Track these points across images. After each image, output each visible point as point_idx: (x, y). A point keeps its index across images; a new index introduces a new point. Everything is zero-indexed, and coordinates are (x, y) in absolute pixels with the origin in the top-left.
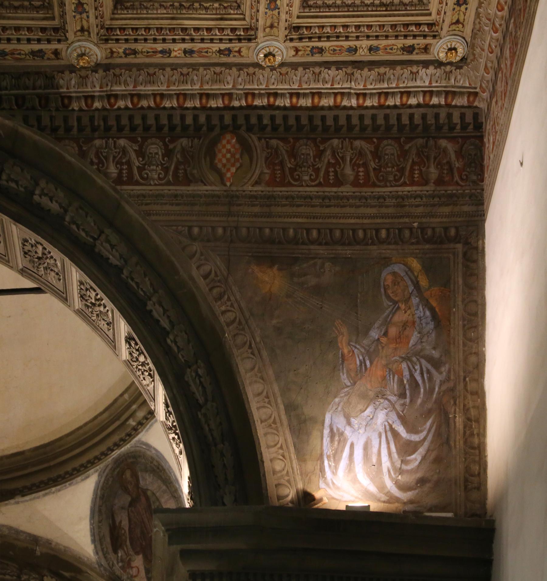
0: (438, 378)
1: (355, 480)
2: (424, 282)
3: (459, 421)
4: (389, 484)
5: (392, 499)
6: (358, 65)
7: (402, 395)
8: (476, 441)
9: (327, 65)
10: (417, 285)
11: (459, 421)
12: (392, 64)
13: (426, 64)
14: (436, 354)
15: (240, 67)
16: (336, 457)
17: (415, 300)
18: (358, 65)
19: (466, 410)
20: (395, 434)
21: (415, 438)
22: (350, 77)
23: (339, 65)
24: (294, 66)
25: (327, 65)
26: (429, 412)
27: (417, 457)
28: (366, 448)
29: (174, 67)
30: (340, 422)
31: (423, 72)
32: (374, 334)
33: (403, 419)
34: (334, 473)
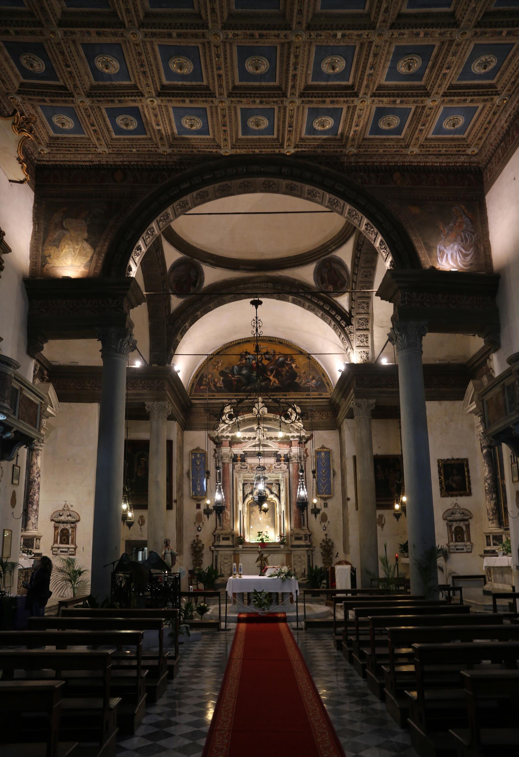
0: (474, 237)
1: (449, 264)
2: (466, 211)
3: (482, 248)
4: (460, 265)
5: (461, 269)
6: (441, 155)
7: (462, 241)
8: (488, 254)
9: (430, 155)
10: (464, 212)
11: (482, 248)
12: (452, 155)
13: (463, 155)
14: (472, 230)
15: (401, 155)
16: (442, 257)
17: (464, 216)
18: (441, 155)
19: (484, 245)
20: (461, 252)
21: (468, 253)
22: (438, 158)
23: (434, 155)
24: (419, 155)
25: (430, 155)
26: (471, 246)
27: (469, 258)
28: (452, 255)
29: (379, 155)
30: (442, 248)
31: (462, 157)
32: (451, 225)
33: (463, 248)
34: (442, 261)
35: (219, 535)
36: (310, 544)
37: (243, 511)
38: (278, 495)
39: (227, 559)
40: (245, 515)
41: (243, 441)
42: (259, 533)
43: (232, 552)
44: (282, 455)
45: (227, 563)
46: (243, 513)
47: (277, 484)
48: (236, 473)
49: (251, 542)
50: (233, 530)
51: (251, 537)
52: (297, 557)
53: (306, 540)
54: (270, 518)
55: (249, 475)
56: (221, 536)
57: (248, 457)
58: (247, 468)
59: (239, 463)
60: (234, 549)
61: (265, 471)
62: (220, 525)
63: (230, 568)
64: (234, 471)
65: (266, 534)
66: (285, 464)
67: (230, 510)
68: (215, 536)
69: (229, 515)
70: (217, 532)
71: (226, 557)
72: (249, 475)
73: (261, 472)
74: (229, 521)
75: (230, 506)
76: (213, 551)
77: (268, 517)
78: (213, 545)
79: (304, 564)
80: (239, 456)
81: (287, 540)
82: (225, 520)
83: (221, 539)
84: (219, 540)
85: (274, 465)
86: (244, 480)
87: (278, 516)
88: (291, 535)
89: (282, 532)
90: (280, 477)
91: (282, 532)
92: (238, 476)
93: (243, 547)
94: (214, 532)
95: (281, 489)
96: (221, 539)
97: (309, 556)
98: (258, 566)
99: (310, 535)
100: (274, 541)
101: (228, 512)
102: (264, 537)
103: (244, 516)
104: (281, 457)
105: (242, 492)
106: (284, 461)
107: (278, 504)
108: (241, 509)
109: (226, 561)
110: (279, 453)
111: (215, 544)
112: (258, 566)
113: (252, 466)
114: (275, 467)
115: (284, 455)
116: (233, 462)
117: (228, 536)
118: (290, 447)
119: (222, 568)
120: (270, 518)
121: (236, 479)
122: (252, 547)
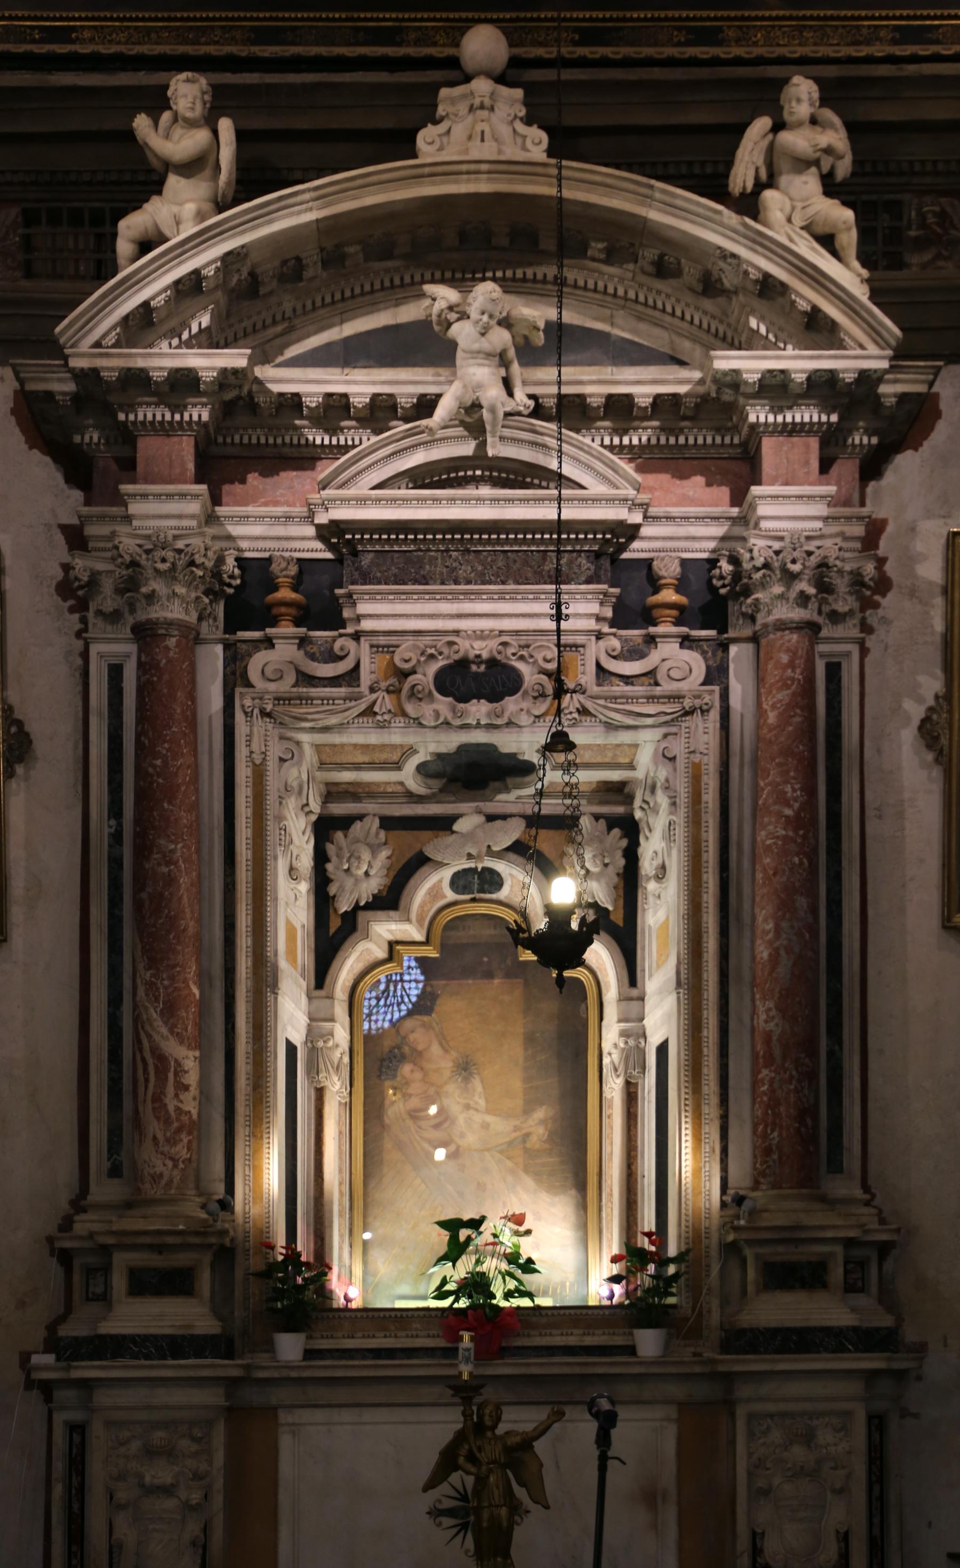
35: (106, 1250)
36: (887, 1321)
37: (314, 1053)
38: (618, 918)
39: (168, 1453)
40: (336, 1087)
41: (318, 438)
42: (452, 1226)
43: (213, 1397)
44: (669, 569)
45: (168, 1490)
46: (313, 1068)
47: (612, 822)
48: (261, 726)
49: (382, 1303)
50: (226, 1205)
51: (383, 1265)
52: (776, 1436)
53: (850, 1288)
54: (540, 1113)
55: (373, 738)
56: (121, 1260)
57: (366, 578)
58: (352, 676)
59: (287, 629)
60: (230, 1368)
61: (511, 704)
62: (115, 1172)
63: (193, 1528)
64: (244, 700)
65: (508, 1240)
66: (686, 642)
67: (200, 1042)
68: (65, 1258)
69: (192, 1078)
70: (84, 1224)
71: (159, 1435)
72: (373, 738)
73: (479, 710)
74: (197, 1128)
75: (204, 1006)
76: (47, 1389)
77: (528, 1110)
78: (52, 1344)
79: (839, 1492)
80: (285, 573)
81: (695, 1290)
82: (154, 1127)
83: (119, 1282)
84: (105, 1298)
85: (594, 651)
86: (332, 793)
87: (614, 1088)
88: (731, 1250)
89: (648, 1221)
90: (645, 758)
91: (648, 1221)
92: (276, 750)
93: (310, 1354)
94: (66, 1225)
95: (647, 865)
96: (119, 1282)
97: (877, 1423)
98: (436, 1513)
99: (884, 1249)
100: (570, 1298)
101: (190, 1060)
102: (491, 1265)
103: (320, 1094)
104: (655, 584)
105: (304, 887)
106: (682, 616)
107: (611, 994)
108: (298, 1038)
109: (161, 1473)
110: (637, 550)
111: (65, 1331)
112: (436, 1513)
113: (405, 653)
114: (602, 672)
115: (684, 563)
116: (231, 626)
117: (181, 1260)
118: (738, 498)
119: (125, 1530)
120: (540, 1113)
121: (259, 774)
122: (390, 1353)
